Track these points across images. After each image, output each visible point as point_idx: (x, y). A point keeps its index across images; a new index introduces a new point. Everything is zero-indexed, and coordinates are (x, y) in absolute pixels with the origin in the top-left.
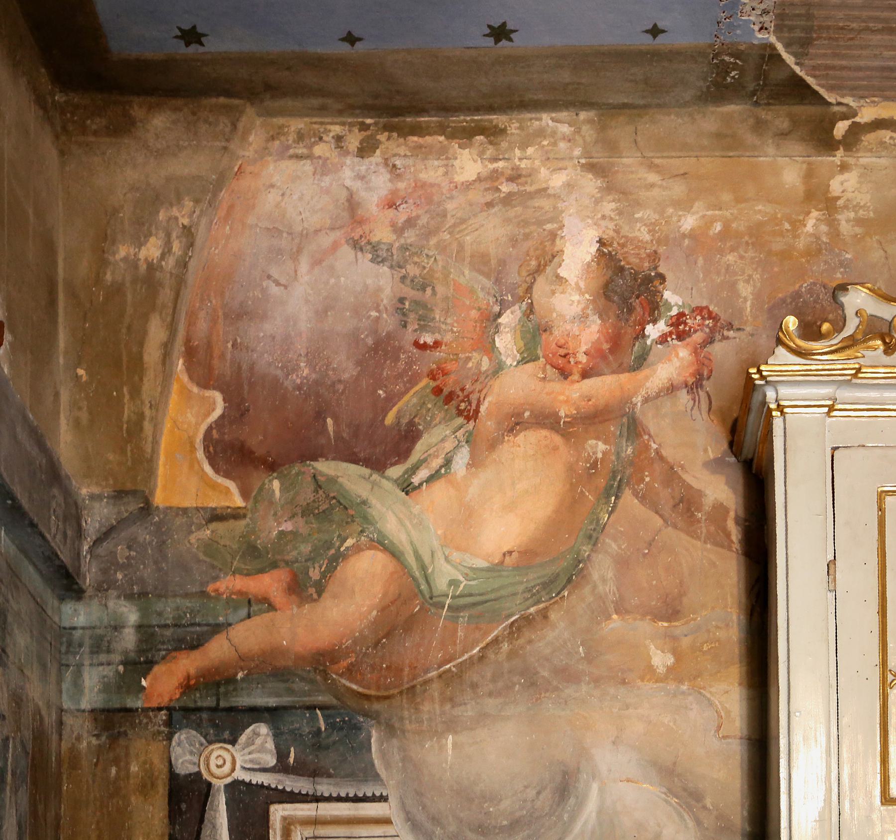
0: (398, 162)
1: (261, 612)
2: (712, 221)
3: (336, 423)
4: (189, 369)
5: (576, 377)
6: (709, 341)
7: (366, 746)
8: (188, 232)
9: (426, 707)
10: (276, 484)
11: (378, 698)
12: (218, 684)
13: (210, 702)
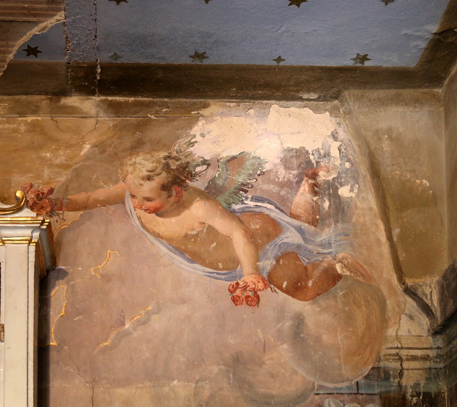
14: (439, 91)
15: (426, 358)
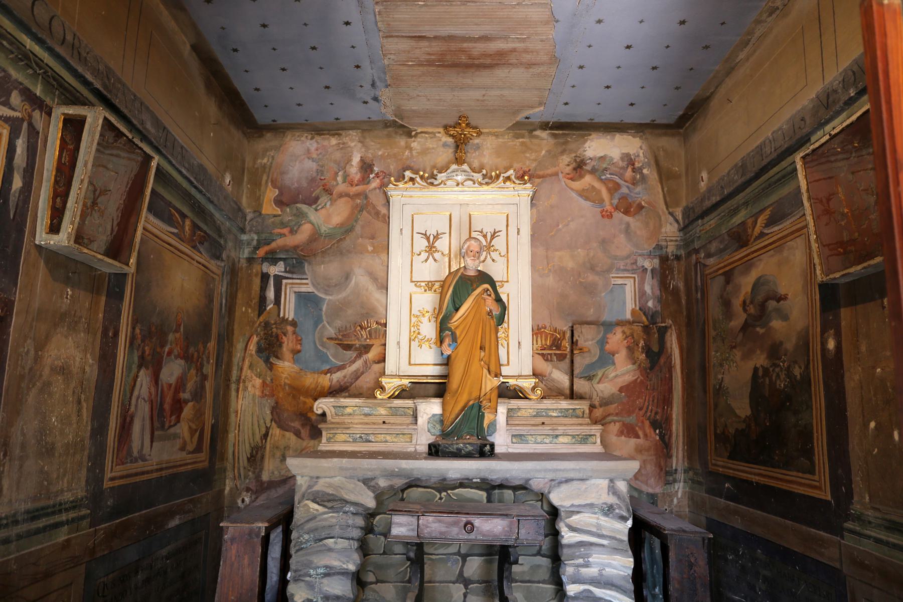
2: (385, 153)
3: (302, 196)
6: (384, 178)
7: (304, 267)
8: (273, 157)
9: (318, 258)
10: (288, 209)
13: (271, 257)
14: (681, 131)
15: (676, 241)
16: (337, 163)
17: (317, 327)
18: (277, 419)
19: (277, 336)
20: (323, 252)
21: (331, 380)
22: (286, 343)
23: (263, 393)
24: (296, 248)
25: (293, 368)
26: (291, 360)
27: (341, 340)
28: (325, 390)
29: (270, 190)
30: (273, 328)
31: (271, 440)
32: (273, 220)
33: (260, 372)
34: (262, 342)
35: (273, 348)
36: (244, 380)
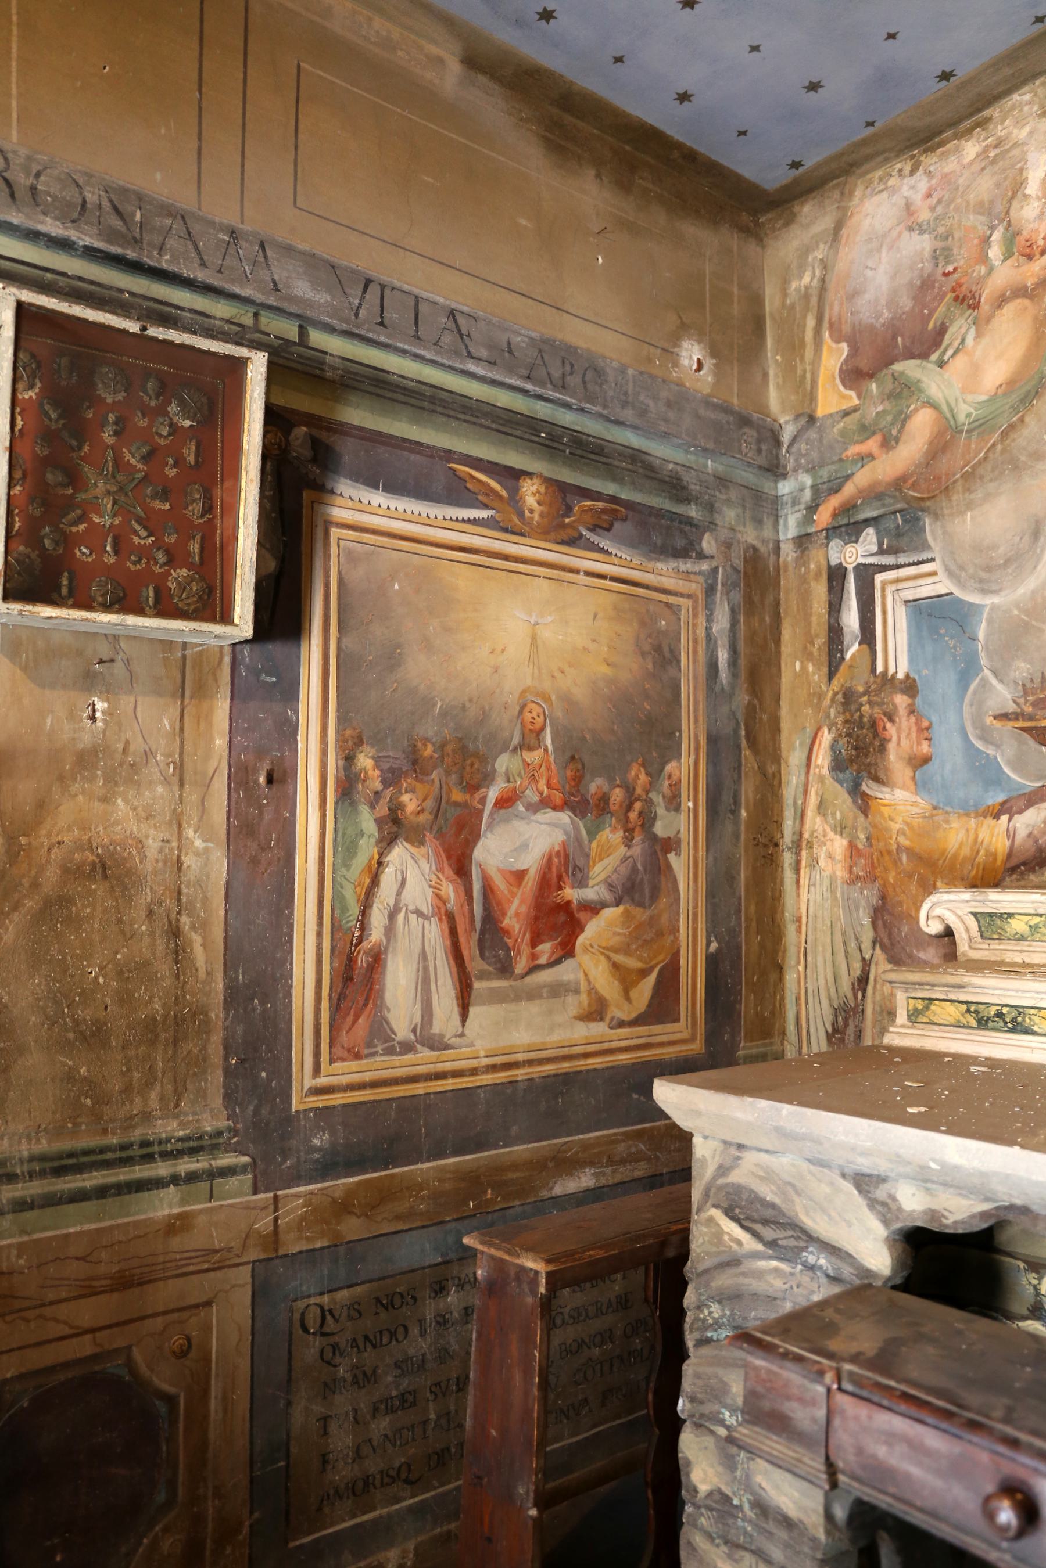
0: (932, 169)
1: (869, 462)
3: (903, 339)
4: (831, 336)
5: (1038, 256)
7: (923, 530)
9: (955, 498)
10: (874, 386)
11: (929, 498)
12: (849, 510)
13: (845, 521)
16: (983, 208)
17: (966, 688)
18: (886, 941)
19: (873, 724)
20: (966, 476)
21: (1011, 835)
22: (895, 739)
23: (851, 872)
24: (899, 483)
25: (914, 804)
26: (910, 783)
27: (1031, 718)
28: (999, 863)
29: (830, 348)
30: (861, 705)
31: (874, 993)
32: (842, 424)
33: (842, 820)
34: (840, 743)
35: (866, 756)
36: (808, 842)
